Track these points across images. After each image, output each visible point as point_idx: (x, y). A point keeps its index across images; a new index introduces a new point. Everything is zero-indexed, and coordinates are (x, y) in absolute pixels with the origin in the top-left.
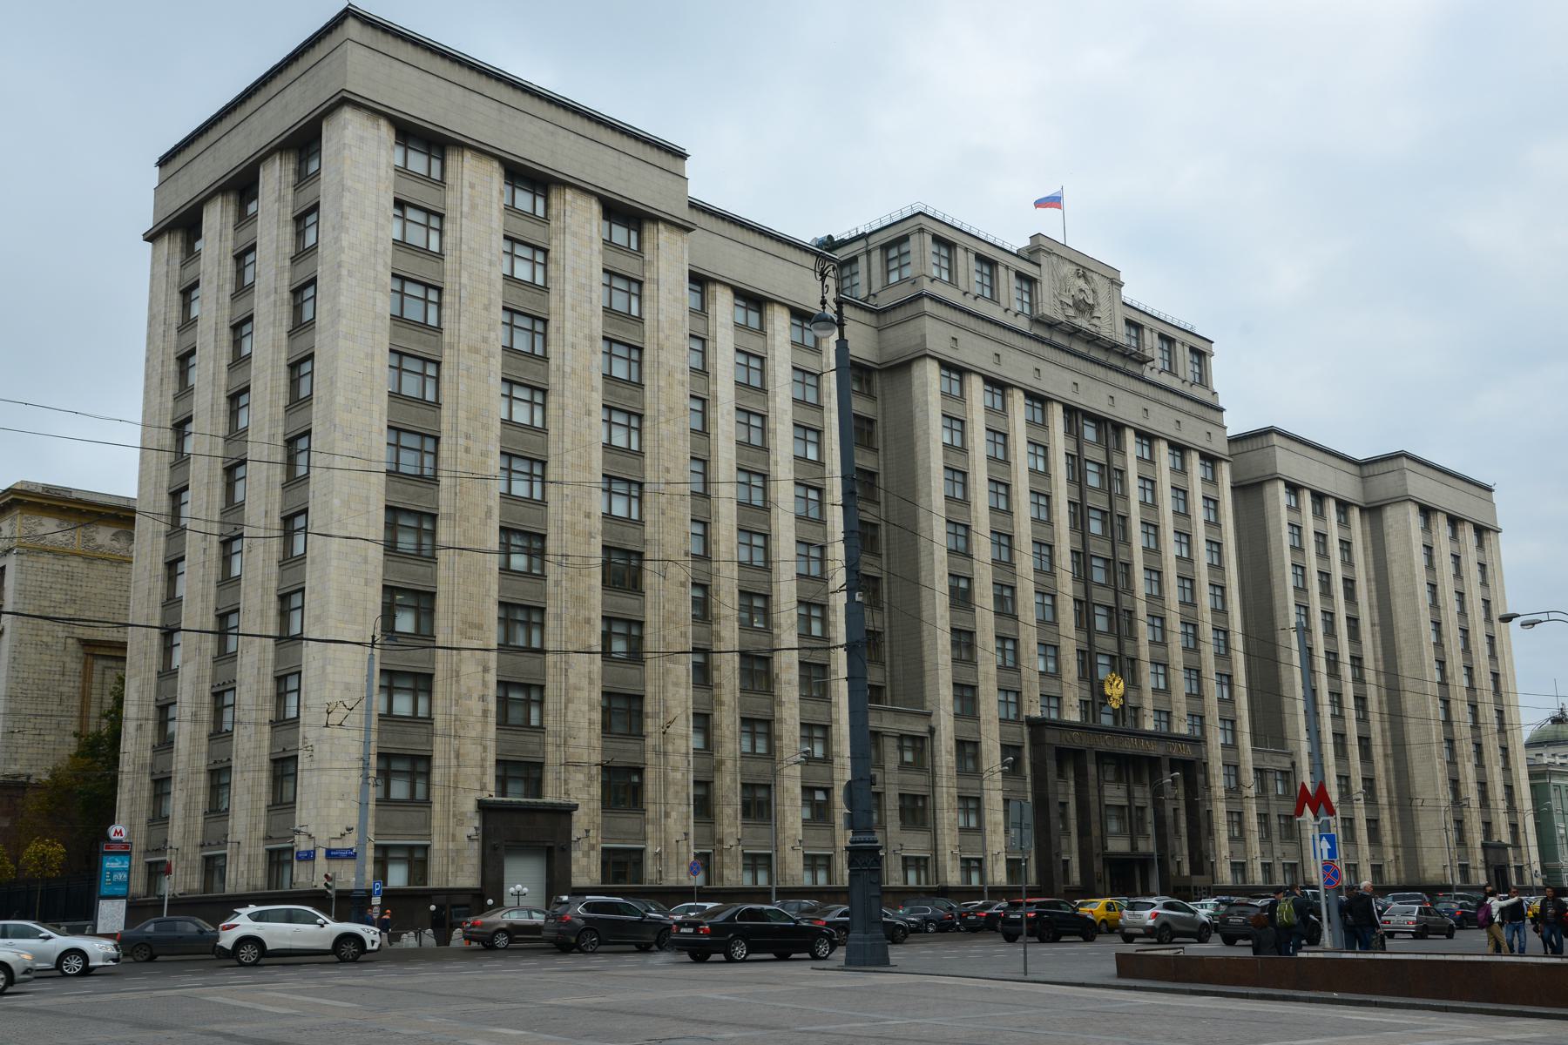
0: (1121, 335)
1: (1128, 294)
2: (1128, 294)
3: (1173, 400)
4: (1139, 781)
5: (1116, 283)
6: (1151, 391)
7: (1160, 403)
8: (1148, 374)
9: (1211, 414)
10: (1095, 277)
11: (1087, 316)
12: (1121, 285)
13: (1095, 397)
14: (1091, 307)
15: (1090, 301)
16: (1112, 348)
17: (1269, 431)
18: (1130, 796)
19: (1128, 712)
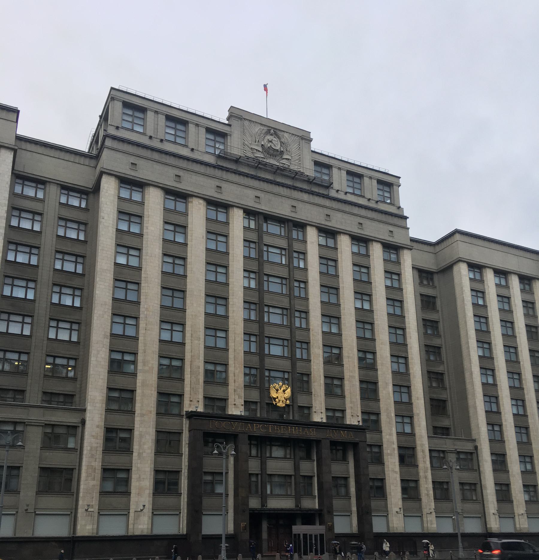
0: (309, 170)
1: (314, 146)
2: (314, 146)
3: (356, 210)
4: (308, 457)
5: (305, 138)
6: (335, 205)
7: (338, 210)
8: (333, 193)
9: (396, 221)
10: (286, 135)
11: (278, 158)
12: (311, 140)
13: (281, 206)
14: (282, 153)
15: (278, 147)
16: (310, 181)
17: (457, 232)
18: (296, 468)
19: (296, 409)
